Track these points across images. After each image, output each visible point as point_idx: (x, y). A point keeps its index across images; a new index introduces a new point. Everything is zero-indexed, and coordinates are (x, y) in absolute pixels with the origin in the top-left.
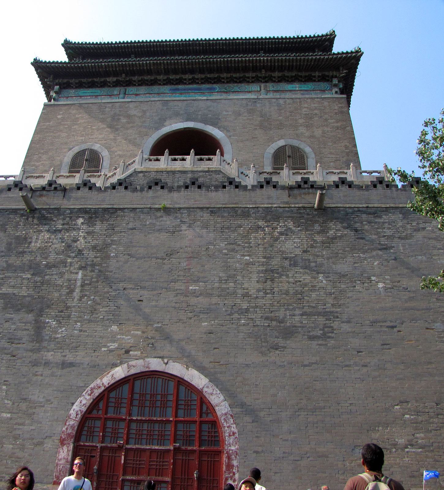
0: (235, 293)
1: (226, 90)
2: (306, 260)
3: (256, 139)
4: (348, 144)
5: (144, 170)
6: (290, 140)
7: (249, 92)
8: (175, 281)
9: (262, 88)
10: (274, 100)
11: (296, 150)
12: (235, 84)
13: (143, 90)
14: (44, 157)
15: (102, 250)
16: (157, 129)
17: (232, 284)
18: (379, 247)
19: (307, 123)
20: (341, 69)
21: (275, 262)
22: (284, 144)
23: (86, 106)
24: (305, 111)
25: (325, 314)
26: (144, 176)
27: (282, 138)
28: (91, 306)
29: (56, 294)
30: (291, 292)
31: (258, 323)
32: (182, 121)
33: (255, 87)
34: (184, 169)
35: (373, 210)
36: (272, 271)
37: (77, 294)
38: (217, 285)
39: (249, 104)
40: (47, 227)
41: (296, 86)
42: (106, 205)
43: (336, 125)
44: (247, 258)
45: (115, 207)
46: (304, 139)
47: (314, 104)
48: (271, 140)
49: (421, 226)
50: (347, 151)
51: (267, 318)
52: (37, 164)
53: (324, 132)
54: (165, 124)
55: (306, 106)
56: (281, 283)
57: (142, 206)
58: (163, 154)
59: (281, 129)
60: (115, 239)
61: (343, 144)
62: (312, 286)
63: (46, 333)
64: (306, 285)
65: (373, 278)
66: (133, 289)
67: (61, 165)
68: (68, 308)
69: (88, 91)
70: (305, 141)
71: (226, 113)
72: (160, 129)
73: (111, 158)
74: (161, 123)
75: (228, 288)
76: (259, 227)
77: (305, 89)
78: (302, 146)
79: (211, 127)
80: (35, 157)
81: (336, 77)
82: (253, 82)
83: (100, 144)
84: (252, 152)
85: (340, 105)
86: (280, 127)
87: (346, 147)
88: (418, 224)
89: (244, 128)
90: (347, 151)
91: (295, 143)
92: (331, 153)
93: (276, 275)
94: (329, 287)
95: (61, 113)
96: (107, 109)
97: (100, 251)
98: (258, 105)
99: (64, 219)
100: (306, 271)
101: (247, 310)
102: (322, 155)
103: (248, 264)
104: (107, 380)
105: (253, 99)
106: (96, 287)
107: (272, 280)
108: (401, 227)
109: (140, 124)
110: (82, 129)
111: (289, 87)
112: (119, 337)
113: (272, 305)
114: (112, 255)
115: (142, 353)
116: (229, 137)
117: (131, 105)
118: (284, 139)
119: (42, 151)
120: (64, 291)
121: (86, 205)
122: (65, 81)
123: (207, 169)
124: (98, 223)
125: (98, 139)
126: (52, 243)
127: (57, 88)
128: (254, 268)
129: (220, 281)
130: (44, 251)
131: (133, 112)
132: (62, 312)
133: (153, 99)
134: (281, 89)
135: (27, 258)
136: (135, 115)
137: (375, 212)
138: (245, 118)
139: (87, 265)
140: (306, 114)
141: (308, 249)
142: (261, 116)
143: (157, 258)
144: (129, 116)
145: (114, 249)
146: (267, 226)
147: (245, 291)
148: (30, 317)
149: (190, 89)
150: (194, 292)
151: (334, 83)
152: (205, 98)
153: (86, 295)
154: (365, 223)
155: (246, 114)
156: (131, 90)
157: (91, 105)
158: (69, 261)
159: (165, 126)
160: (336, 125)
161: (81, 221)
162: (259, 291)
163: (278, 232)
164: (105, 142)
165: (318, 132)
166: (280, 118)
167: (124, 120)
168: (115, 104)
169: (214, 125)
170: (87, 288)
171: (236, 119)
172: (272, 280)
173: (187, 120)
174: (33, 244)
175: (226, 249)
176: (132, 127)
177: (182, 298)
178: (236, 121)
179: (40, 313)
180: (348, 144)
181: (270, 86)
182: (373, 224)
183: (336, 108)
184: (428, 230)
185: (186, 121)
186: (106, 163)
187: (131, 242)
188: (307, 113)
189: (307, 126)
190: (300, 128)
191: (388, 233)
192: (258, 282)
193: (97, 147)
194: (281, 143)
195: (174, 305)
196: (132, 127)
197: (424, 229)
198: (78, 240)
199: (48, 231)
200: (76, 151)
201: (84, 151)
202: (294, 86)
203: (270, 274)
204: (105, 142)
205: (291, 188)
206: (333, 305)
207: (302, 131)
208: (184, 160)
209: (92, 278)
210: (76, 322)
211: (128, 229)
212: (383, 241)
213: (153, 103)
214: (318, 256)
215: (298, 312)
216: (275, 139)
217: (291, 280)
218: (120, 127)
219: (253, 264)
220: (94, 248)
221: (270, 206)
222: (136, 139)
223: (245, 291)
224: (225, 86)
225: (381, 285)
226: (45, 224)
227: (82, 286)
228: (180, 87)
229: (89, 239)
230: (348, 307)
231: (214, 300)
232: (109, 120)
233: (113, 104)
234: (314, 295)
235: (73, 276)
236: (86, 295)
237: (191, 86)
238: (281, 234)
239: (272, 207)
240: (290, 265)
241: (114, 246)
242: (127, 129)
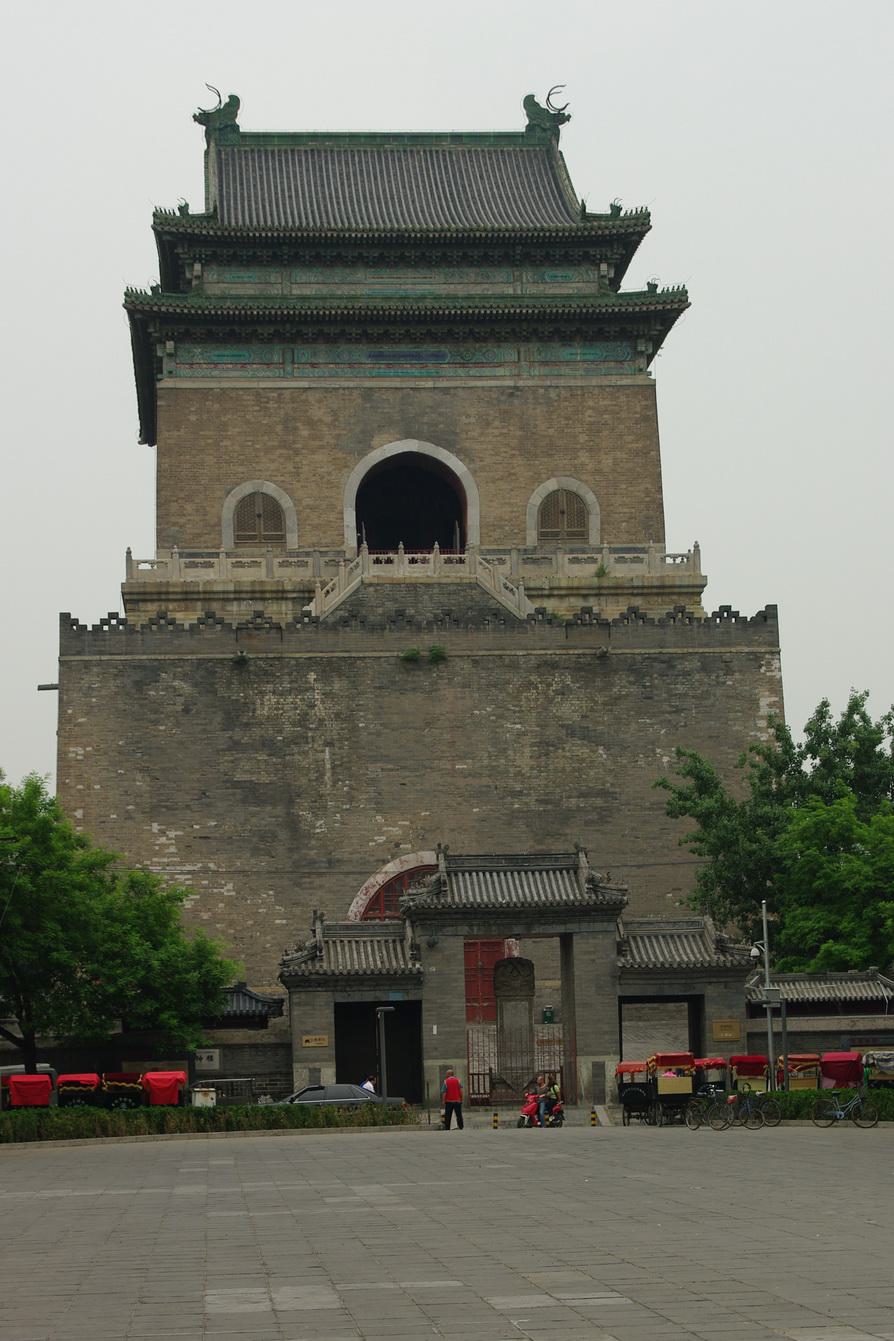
0: (508, 772)
1: (462, 358)
2: (584, 728)
3: (514, 477)
4: (649, 486)
5: (376, 581)
6: (564, 479)
7: (500, 365)
8: (440, 759)
9: (522, 359)
10: (542, 391)
11: (574, 497)
12: (477, 345)
13: (322, 353)
14: (189, 507)
15: (347, 718)
16: (363, 454)
17: (503, 761)
18: (669, 709)
19: (591, 443)
20: (653, 322)
21: (551, 733)
22: (556, 488)
23: (233, 394)
24: (590, 416)
25: (603, 793)
26: (376, 591)
27: (552, 474)
28: (348, 793)
29: (304, 781)
30: (568, 769)
31: (533, 807)
32: (398, 436)
33: (508, 353)
34: (429, 581)
35: (666, 658)
36: (547, 744)
37: (328, 776)
38: (486, 762)
39: (503, 398)
40: (270, 687)
41: (576, 352)
42: (341, 651)
43: (635, 445)
44: (519, 726)
45: (354, 655)
46: (584, 477)
47: (604, 399)
48: (537, 479)
49: (721, 679)
50: (648, 499)
51: (540, 801)
52: (182, 521)
53: (615, 459)
54: (375, 441)
55: (591, 403)
56: (557, 758)
57: (388, 654)
58: (396, 550)
59: (551, 456)
60: (361, 702)
61: (642, 487)
62: (591, 762)
63: (303, 826)
64: (583, 760)
65: (658, 751)
66: (392, 770)
67: (218, 524)
68: (321, 796)
69: (226, 353)
70: (586, 481)
71: (467, 421)
72: (366, 455)
73: (298, 513)
74: (364, 446)
75: (499, 767)
76: (531, 683)
77: (591, 357)
78: (581, 492)
79: (446, 452)
80: (174, 507)
81: (643, 336)
82: (506, 340)
83: (275, 482)
84: (509, 504)
85: (643, 403)
86: (550, 453)
87: (647, 493)
88: (717, 677)
89: (496, 454)
90: (648, 499)
91: (573, 484)
92: (623, 505)
93: (551, 748)
94: (609, 762)
96: (272, 405)
97: (344, 720)
98: (516, 402)
99: (290, 674)
100: (585, 742)
101: (520, 793)
102: (612, 508)
103: (520, 734)
104: (380, 879)
105: (509, 387)
106: (349, 769)
107: (547, 755)
108: (697, 681)
109: (333, 441)
110: (237, 448)
111: (565, 353)
112: (385, 829)
113: (547, 786)
114: (361, 725)
115: (413, 846)
116: (474, 472)
117: (311, 397)
118: (555, 476)
119: (182, 495)
120: (313, 776)
121: (314, 652)
122: (182, 329)
123: (458, 581)
124: (336, 679)
125: (269, 473)
126: (282, 709)
127: (170, 345)
128: (527, 740)
129: (490, 757)
130: (273, 720)
131: (318, 413)
132: (315, 802)
133: (346, 384)
134: (553, 359)
135: (257, 732)
136: (320, 420)
137: (669, 662)
138: (496, 432)
139: (333, 739)
140: (591, 424)
141: (588, 713)
142: (521, 428)
143: (416, 729)
144: (311, 423)
145: (362, 716)
146: (540, 683)
147: (518, 769)
148: (280, 810)
149: (403, 356)
150: (462, 771)
151: (639, 349)
152: (430, 384)
153: (339, 780)
154: (655, 676)
155: (497, 423)
156: (304, 353)
157: (241, 392)
158: (310, 735)
159: (373, 449)
160: (635, 445)
161: (312, 676)
162: (532, 768)
163: (553, 691)
164: (282, 478)
165: (607, 462)
166: (551, 431)
167: (305, 432)
168: (284, 391)
169: (449, 446)
170: (338, 770)
171: (482, 434)
172: (547, 755)
173: (408, 435)
174: (259, 712)
175: (493, 715)
176: (322, 447)
177: (449, 780)
178: (482, 439)
179: (291, 802)
180: (649, 486)
181: (534, 346)
182: (665, 678)
183: (638, 409)
184: (729, 686)
185: (406, 438)
186: (291, 521)
187: (381, 708)
188: (592, 419)
189: (591, 450)
190: (580, 454)
191: (681, 688)
192: (531, 757)
193: (270, 488)
194: (552, 485)
195: (440, 788)
196: (322, 447)
197: (724, 683)
198: (316, 706)
199: (274, 693)
200: (240, 497)
201: (252, 496)
202: (574, 351)
203: (545, 747)
204: (282, 478)
205: (569, 625)
206: (612, 784)
207: (583, 459)
208: (424, 561)
209: (342, 757)
210: (335, 813)
211: (375, 688)
212: (676, 702)
213: (347, 392)
214: (598, 723)
215: (575, 793)
216: (544, 476)
217: (568, 754)
218: (299, 446)
219: (524, 734)
220: (337, 715)
221: (543, 652)
222: (329, 474)
223: (518, 769)
224: (462, 350)
225: (665, 759)
226: (268, 682)
227: (333, 768)
228: (386, 348)
229: (329, 704)
230: (628, 787)
231: (485, 781)
232: (279, 428)
233: (279, 391)
234: (592, 773)
235: (320, 755)
236: (339, 780)
237: (404, 348)
238: (557, 692)
239: (546, 654)
240: (567, 735)
241: (362, 714)
242: (313, 452)
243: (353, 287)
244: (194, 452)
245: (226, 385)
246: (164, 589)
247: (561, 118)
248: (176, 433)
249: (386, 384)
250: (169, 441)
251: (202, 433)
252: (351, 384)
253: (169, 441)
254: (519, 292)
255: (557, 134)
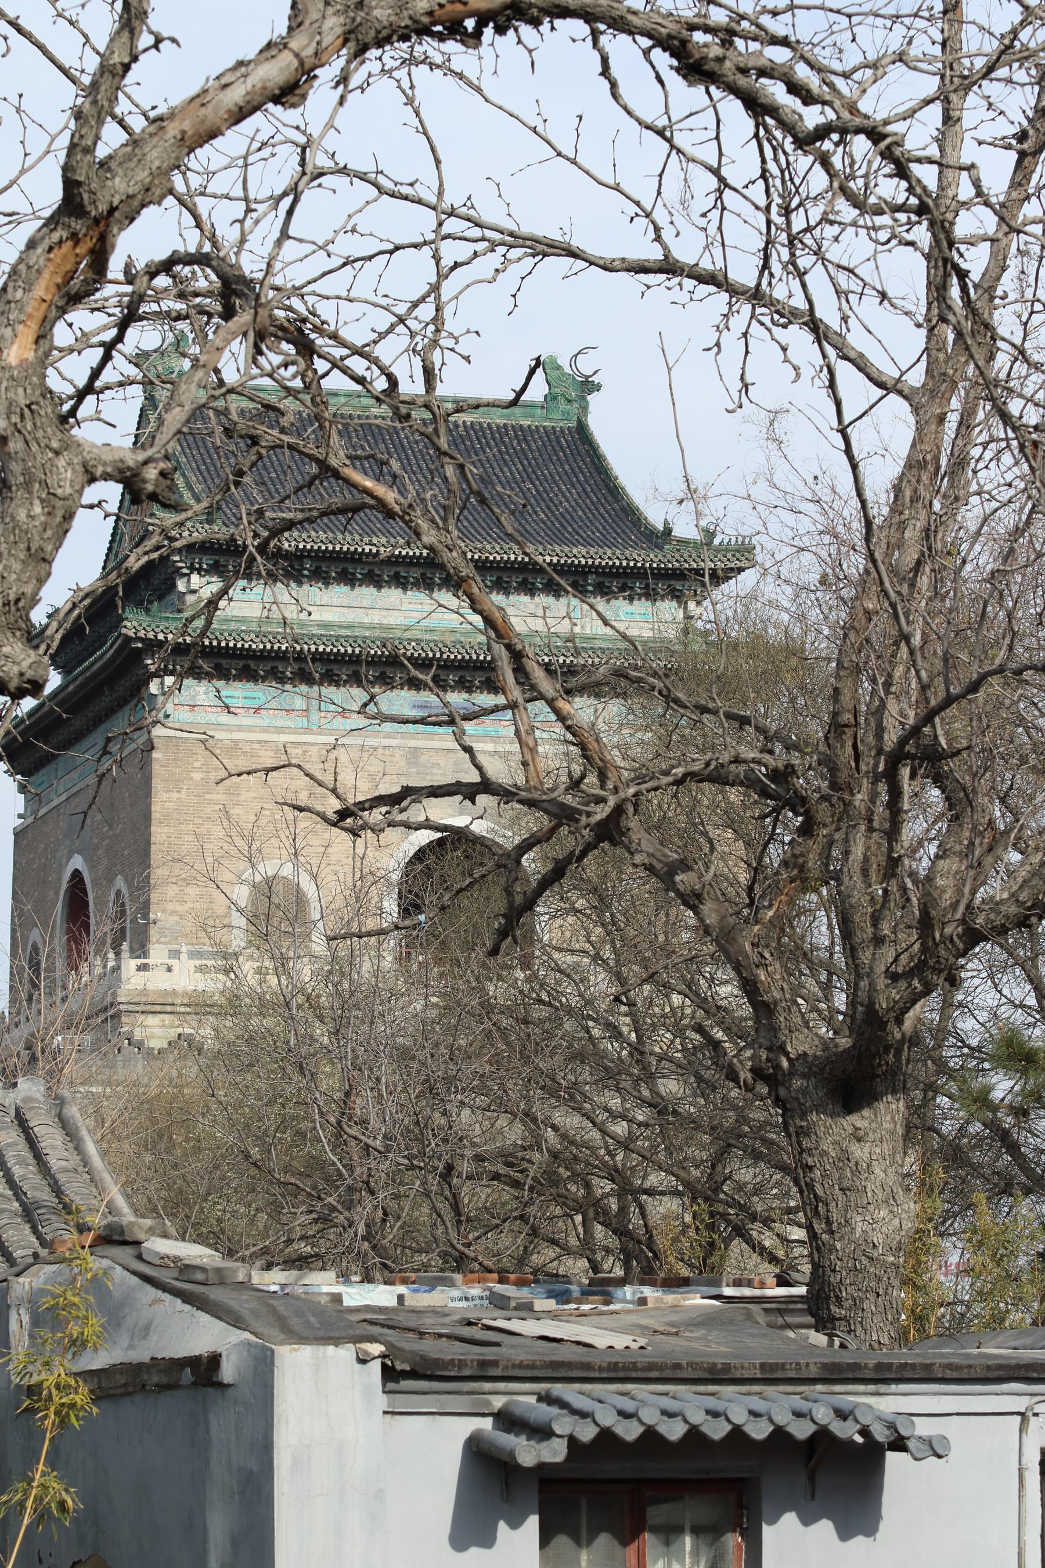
32: (452, 812)
95: (197, 765)
127: (169, 680)
157: (257, 746)
243: (385, 613)
244: (196, 821)
245: (237, 736)
246: (170, 1001)
247: (588, 386)
248: (175, 795)
249: (436, 744)
250: (166, 805)
251: (207, 796)
252: (394, 742)
253: (166, 805)
254: (588, 631)
255: (584, 408)
